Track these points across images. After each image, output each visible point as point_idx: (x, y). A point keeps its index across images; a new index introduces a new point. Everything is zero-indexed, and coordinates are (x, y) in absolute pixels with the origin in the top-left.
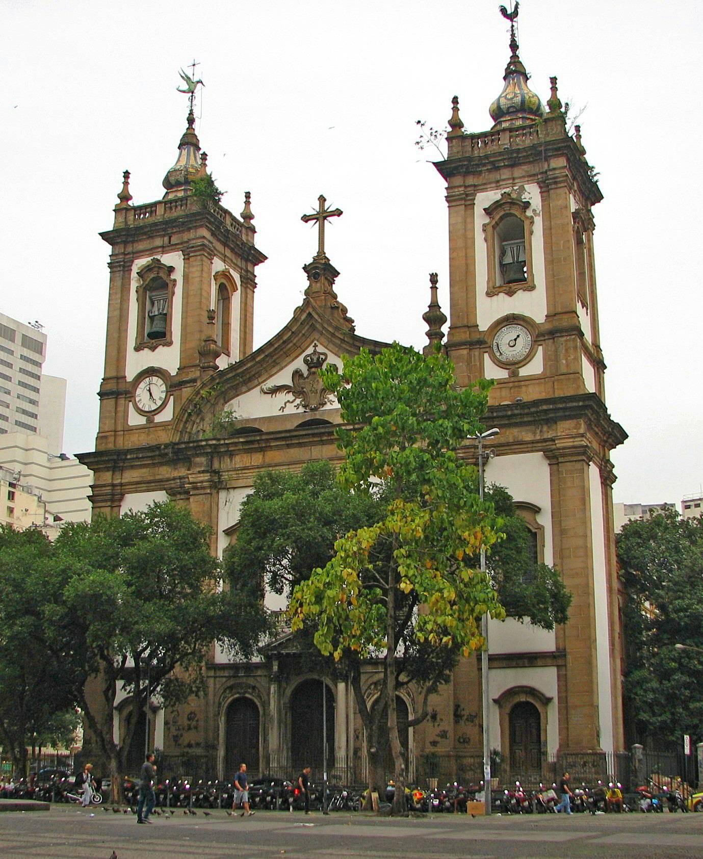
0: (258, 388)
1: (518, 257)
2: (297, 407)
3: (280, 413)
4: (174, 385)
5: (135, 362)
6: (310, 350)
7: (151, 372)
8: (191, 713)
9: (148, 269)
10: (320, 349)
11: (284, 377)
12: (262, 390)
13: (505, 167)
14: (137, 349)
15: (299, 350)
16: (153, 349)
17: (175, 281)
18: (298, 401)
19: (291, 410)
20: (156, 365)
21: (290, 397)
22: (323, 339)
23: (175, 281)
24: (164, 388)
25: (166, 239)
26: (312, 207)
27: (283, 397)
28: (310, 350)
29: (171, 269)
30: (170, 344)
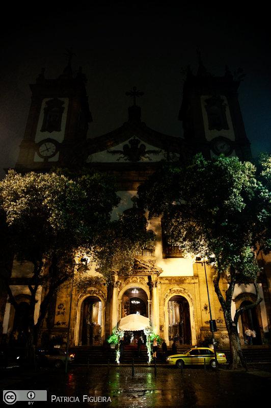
2: (126, 160)
3: (117, 162)
4: (58, 146)
6: (132, 138)
8: (61, 305)
10: (137, 138)
11: (120, 147)
14: (43, 130)
17: (64, 108)
18: (125, 158)
19: (122, 161)
21: (122, 155)
24: (55, 148)
27: (118, 156)
28: (132, 138)
30: (60, 130)
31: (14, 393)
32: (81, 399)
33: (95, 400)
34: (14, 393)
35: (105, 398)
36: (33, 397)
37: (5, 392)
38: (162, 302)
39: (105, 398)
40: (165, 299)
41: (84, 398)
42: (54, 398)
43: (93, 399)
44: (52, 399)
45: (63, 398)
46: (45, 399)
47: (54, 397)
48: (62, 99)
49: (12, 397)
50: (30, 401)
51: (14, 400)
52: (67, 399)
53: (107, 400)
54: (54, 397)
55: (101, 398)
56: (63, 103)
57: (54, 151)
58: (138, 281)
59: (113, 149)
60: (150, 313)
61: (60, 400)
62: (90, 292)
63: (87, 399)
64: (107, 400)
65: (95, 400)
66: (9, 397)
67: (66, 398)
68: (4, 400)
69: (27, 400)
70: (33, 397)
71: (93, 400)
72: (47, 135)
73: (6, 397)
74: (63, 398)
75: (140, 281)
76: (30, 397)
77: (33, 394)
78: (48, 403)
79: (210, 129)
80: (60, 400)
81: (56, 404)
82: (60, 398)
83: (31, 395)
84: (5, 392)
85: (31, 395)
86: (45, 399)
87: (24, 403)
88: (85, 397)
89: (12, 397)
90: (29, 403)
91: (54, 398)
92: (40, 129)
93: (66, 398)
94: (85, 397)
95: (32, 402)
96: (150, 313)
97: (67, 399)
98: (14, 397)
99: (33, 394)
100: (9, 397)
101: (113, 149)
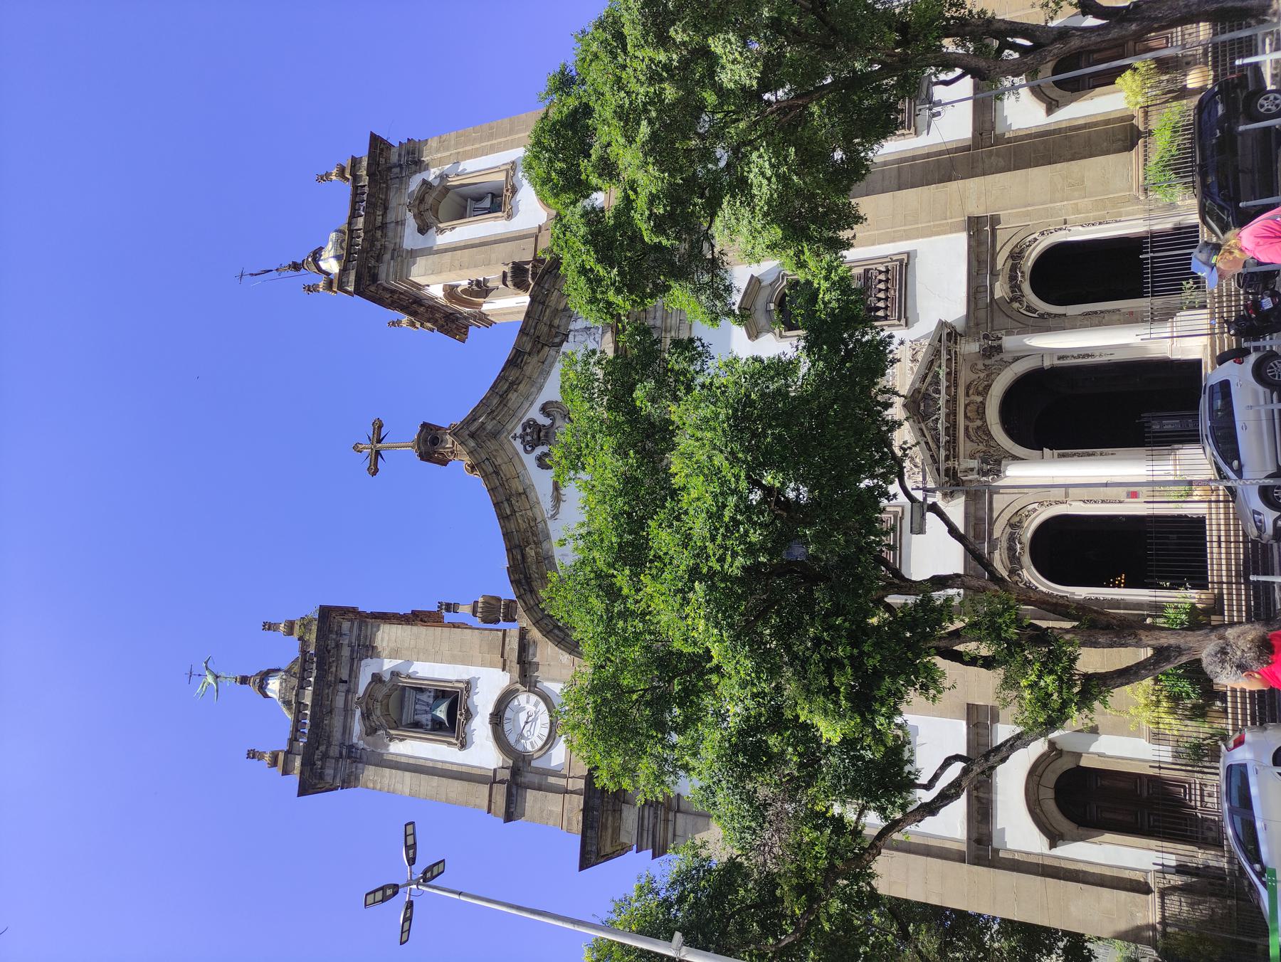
0: (549, 523)
1: (485, 209)
5: (483, 753)
7: (497, 719)
9: (366, 716)
10: (519, 430)
11: (541, 482)
12: (553, 516)
13: (384, 215)
15: (516, 460)
16: (469, 715)
20: (491, 709)
22: (509, 427)
23: (392, 673)
25: (343, 687)
26: (363, 461)
28: (518, 445)
29: (377, 678)
38: (1051, 322)
40: (1042, 316)
48: (364, 680)
56: (377, 678)
57: (534, 698)
58: (979, 399)
59: (546, 502)
60: (1088, 356)
62: (1014, 558)
72: (480, 727)
75: (979, 394)
79: (509, 217)
92: (455, 750)
96: (1088, 356)
101: (546, 502)
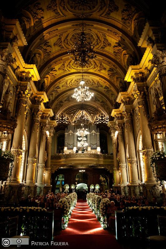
31: (9, 240)
32: (50, 243)
33: (58, 244)
34: (9, 240)
35: (64, 243)
36: (20, 242)
37: (3, 239)
39: (64, 243)
41: (52, 243)
42: (33, 243)
43: (57, 243)
44: (32, 244)
45: (39, 243)
46: (28, 244)
47: (33, 243)
49: (7, 242)
50: (19, 245)
51: (8, 244)
52: (41, 244)
53: (65, 244)
54: (33, 243)
55: (62, 243)
61: (37, 244)
63: (53, 244)
64: (65, 244)
65: (58, 244)
66: (5, 242)
67: (40, 243)
68: (2, 244)
69: (16, 244)
70: (20, 242)
71: (57, 244)
73: (4, 243)
74: (39, 243)
76: (18, 242)
77: (20, 240)
78: (29, 246)
80: (37, 244)
81: (34, 246)
82: (37, 243)
83: (19, 241)
84: (3, 239)
85: (19, 241)
86: (28, 244)
87: (15, 246)
88: (52, 242)
89: (7, 242)
90: (18, 246)
91: (33, 243)
93: (40, 243)
94: (52, 242)
95: (20, 245)
97: (41, 244)
98: (9, 242)
99: (20, 240)
100: (5, 242)
